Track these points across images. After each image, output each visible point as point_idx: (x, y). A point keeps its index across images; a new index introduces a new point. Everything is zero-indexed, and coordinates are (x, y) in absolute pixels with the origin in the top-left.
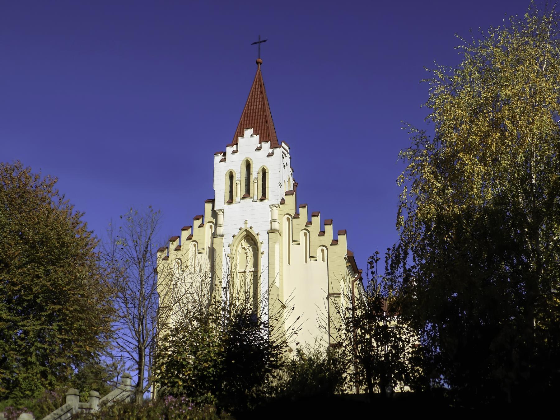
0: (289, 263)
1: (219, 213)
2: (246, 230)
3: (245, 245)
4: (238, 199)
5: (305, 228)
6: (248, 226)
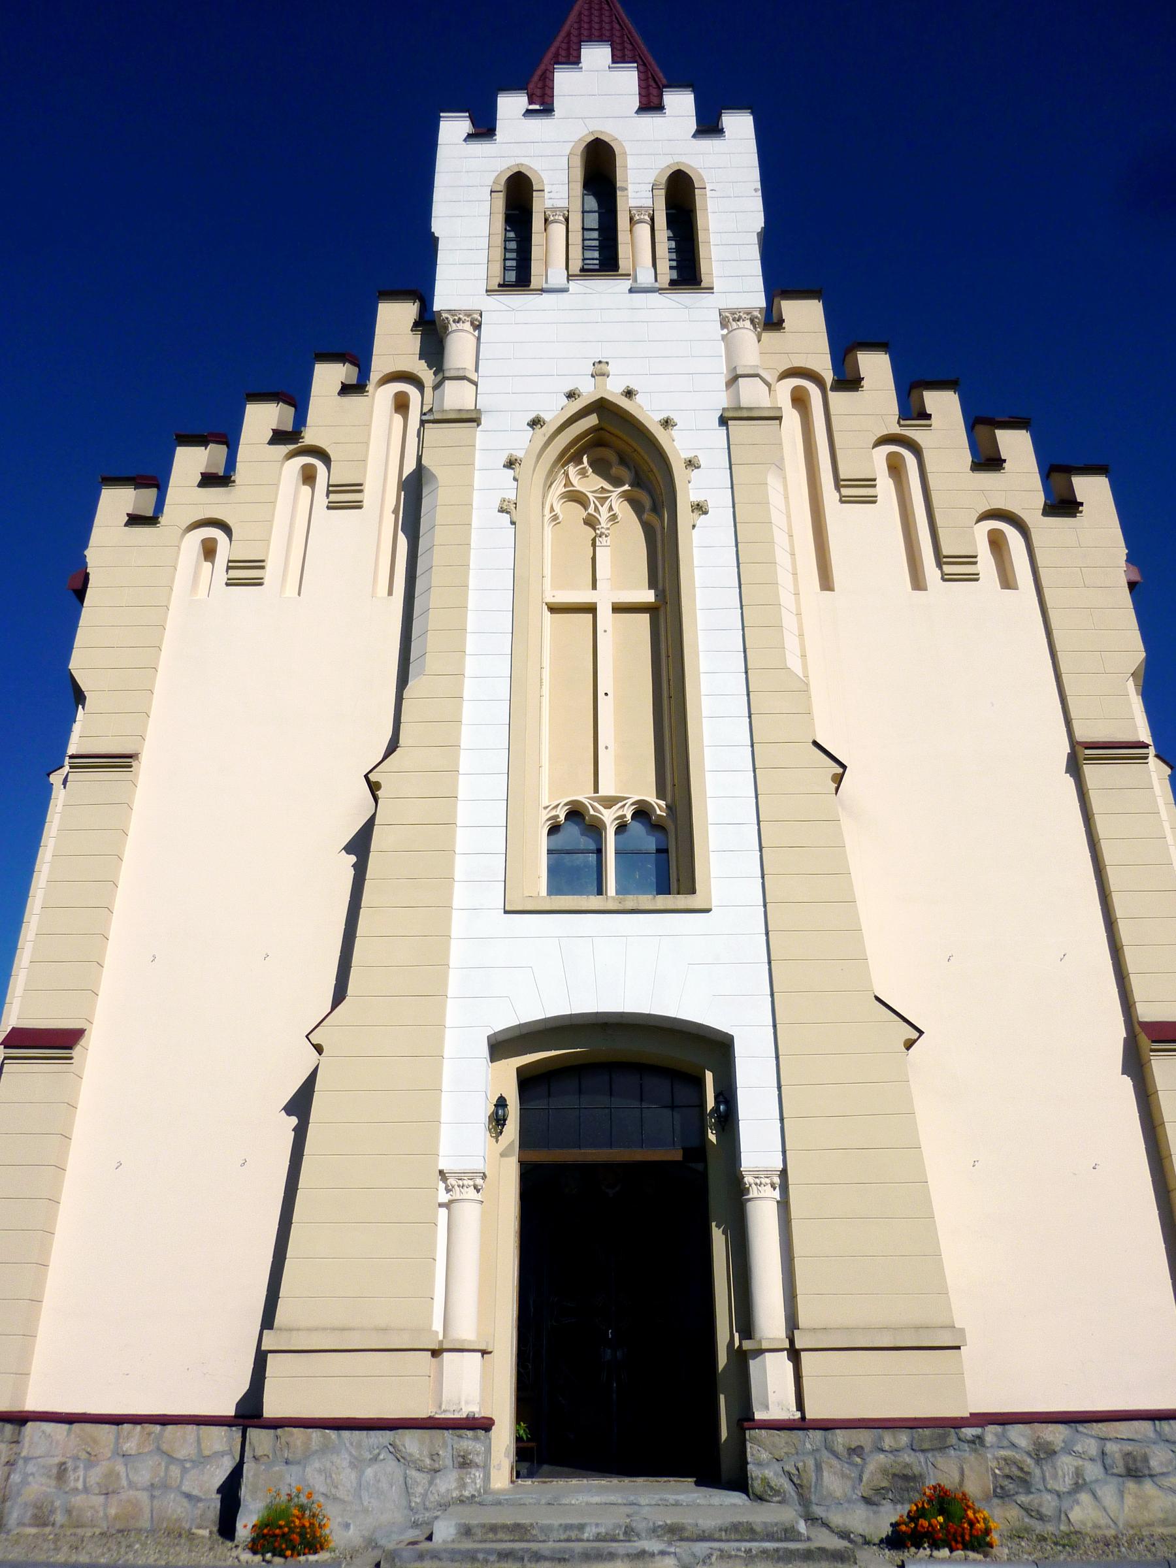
0: (826, 582)
1: (453, 326)
2: (601, 406)
3: (590, 483)
4: (557, 276)
5: (895, 429)
6: (613, 390)
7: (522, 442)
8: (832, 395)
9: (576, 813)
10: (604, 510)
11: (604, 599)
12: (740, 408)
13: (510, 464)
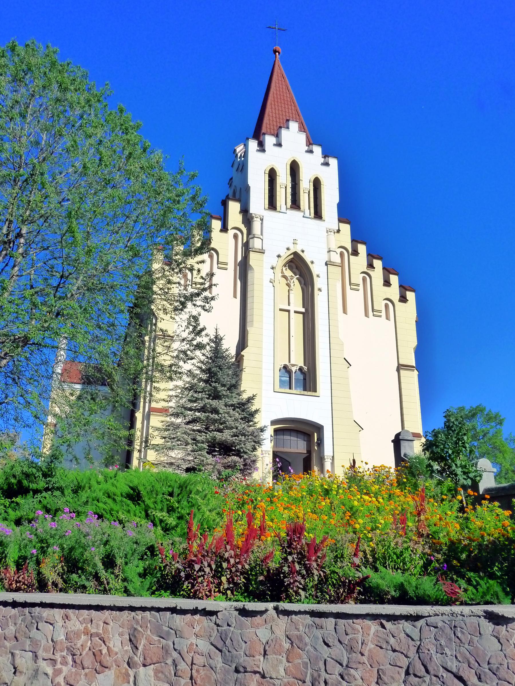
0: (345, 311)
1: (255, 219)
2: (295, 254)
3: (289, 273)
5: (366, 270)
7: (274, 261)
8: (351, 256)
9: (285, 367)
10: (292, 281)
11: (292, 308)
12: (330, 262)
13: (273, 268)
